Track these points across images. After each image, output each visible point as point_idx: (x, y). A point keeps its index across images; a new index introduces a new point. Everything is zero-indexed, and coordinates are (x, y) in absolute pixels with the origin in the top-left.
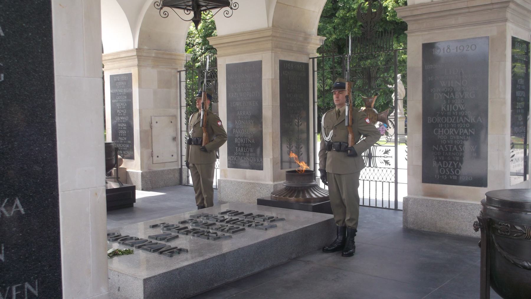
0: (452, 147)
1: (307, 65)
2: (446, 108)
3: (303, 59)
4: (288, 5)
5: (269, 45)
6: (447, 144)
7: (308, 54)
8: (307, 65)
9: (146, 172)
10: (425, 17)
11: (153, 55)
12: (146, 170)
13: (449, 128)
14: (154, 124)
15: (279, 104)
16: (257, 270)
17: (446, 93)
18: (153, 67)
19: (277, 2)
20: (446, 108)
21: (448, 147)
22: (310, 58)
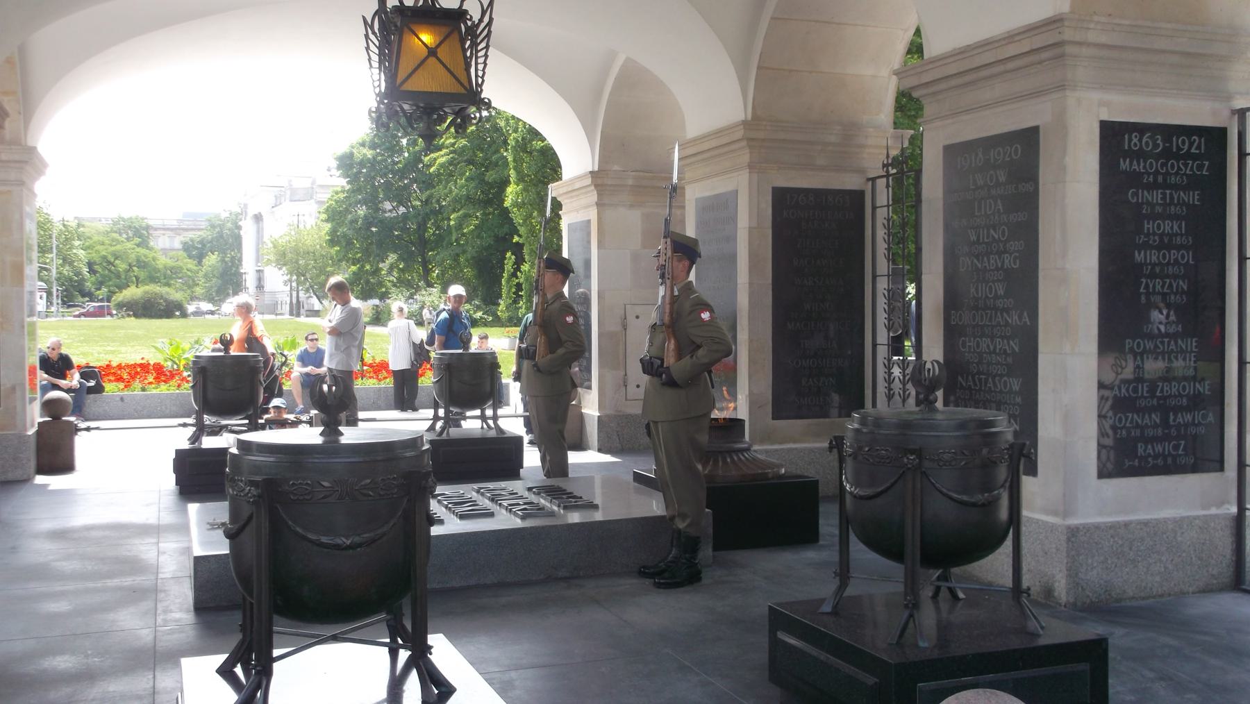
0: (986, 381)
1: (858, 196)
2: (977, 289)
3: (850, 182)
4: (791, 71)
5: (745, 157)
6: (979, 373)
7: (861, 171)
8: (861, 194)
9: (607, 416)
10: (943, 86)
11: (630, 182)
12: (609, 412)
13: (981, 337)
14: (631, 319)
15: (770, 281)
16: (456, 583)
17: (977, 257)
18: (631, 206)
19: (759, 68)
20: (977, 289)
21: (980, 380)
22: (869, 179)
